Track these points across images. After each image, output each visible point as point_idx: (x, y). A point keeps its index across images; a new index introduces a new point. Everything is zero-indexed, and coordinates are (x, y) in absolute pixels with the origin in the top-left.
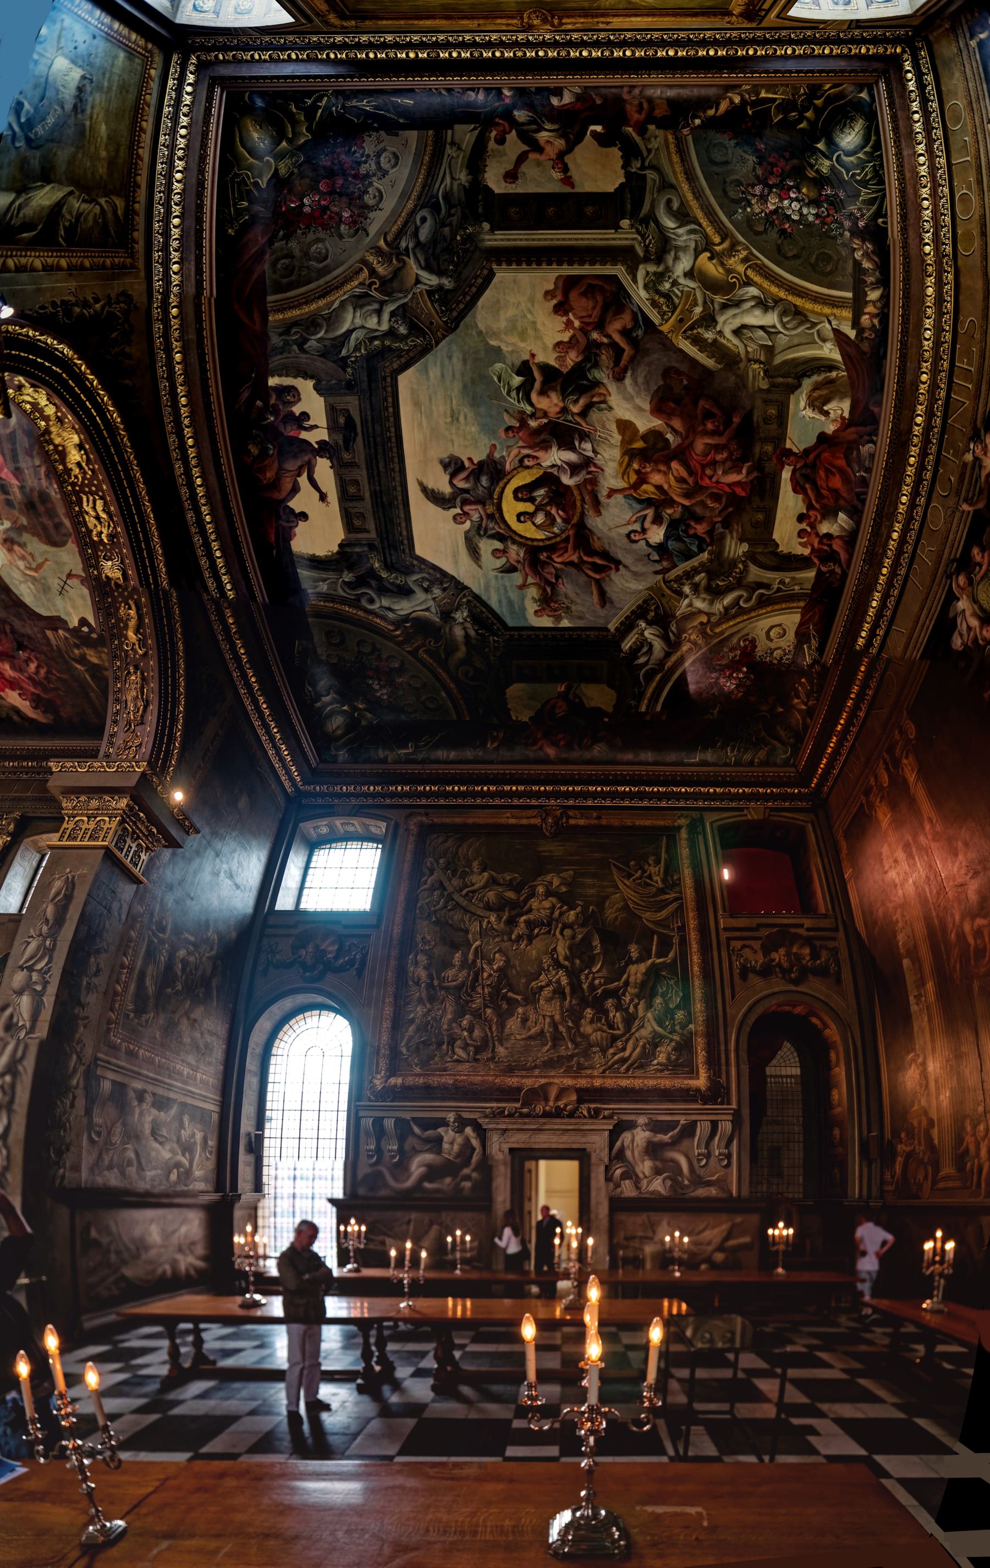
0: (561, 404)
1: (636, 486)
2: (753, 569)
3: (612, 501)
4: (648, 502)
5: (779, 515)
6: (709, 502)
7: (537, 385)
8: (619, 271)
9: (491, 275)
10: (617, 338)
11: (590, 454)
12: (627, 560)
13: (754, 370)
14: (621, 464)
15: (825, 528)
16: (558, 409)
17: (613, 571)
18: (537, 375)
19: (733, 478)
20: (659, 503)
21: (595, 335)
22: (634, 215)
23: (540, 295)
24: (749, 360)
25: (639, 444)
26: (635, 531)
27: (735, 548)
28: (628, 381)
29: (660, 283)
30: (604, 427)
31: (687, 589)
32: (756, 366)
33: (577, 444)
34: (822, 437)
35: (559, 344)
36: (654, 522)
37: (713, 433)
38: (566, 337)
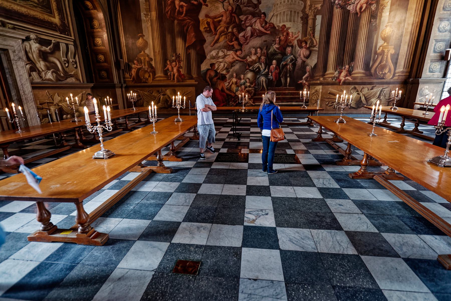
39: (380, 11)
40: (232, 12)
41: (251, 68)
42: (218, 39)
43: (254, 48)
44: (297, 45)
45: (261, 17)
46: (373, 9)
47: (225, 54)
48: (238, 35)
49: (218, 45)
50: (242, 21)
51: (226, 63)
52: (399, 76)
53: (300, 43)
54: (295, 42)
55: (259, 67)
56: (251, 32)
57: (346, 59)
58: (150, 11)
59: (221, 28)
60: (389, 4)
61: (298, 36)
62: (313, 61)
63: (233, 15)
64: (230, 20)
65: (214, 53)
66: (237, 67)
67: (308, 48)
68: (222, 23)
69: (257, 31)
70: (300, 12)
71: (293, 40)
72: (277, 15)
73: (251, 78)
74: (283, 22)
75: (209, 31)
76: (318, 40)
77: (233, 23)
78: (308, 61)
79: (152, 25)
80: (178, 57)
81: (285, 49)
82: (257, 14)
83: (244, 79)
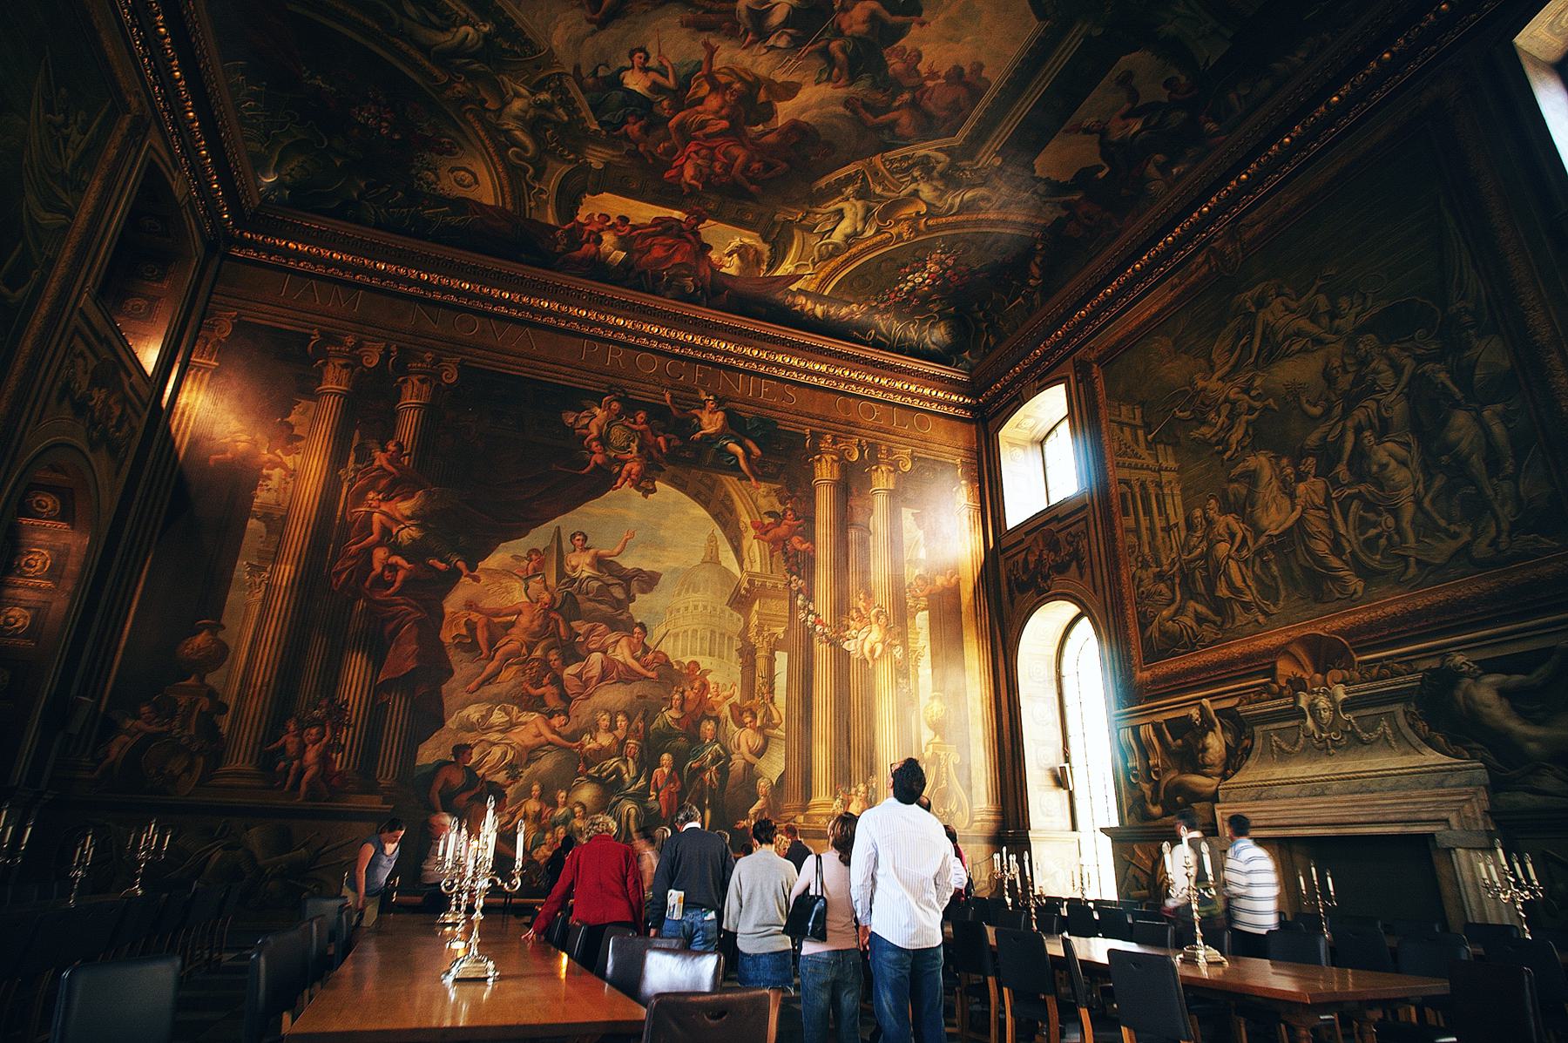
0: (847, 33)
1: (711, 78)
2: (565, 169)
3: (699, 46)
4: (684, 84)
5: (632, 202)
6: (666, 145)
7: (885, 14)
8: (958, 139)
9: (1040, 18)
10: (892, 115)
11: (771, 42)
12: (605, 38)
13: (797, 214)
14: (745, 71)
15: (608, 239)
16: (844, 26)
17: (589, 15)
18: (899, 19)
19: (689, 172)
20: (680, 95)
21: (907, 96)
22: (1000, 168)
23: (983, 59)
24: (807, 213)
25: (762, 96)
26: (647, 59)
27: (596, 158)
28: (841, 109)
29: (922, 170)
30: (799, 68)
31: (545, 96)
32: (799, 216)
33: (789, 31)
34: (711, 248)
35: (919, 56)
36: (654, 83)
37: (746, 168)
38: (922, 67)
39: (912, 662)
40: (550, 607)
41: (591, 771)
42: (496, 674)
43: (607, 711)
44: (730, 719)
45: (633, 633)
46: (898, 656)
47: (510, 721)
48: (563, 670)
49: (493, 689)
50: (579, 635)
51: (513, 748)
52: (982, 820)
53: (738, 712)
54: (725, 710)
55: (617, 771)
56: (603, 668)
57: (857, 766)
58: (274, 562)
59: (513, 642)
60: (928, 650)
61: (731, 696)
62: (773, 767)
63: (552, 615)
64: (540, 626)
65: (474, 713)
66: (547, 763)
67: (760, 730)
68: (514, 630)
69: (620, 667)
70: (735, 638)
71: (719, 704)
72: (676, 635)
73: (588, 805)
74: (691, 654)
75: (469, 646)
76: (783, 711)
77: (553, 635)
78: (762, 764)
79: (266, 603)
80: (337, 713)
81: (698, 724)
82: (622, 624)
83: (565, 804)
